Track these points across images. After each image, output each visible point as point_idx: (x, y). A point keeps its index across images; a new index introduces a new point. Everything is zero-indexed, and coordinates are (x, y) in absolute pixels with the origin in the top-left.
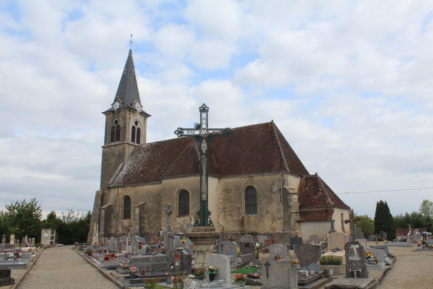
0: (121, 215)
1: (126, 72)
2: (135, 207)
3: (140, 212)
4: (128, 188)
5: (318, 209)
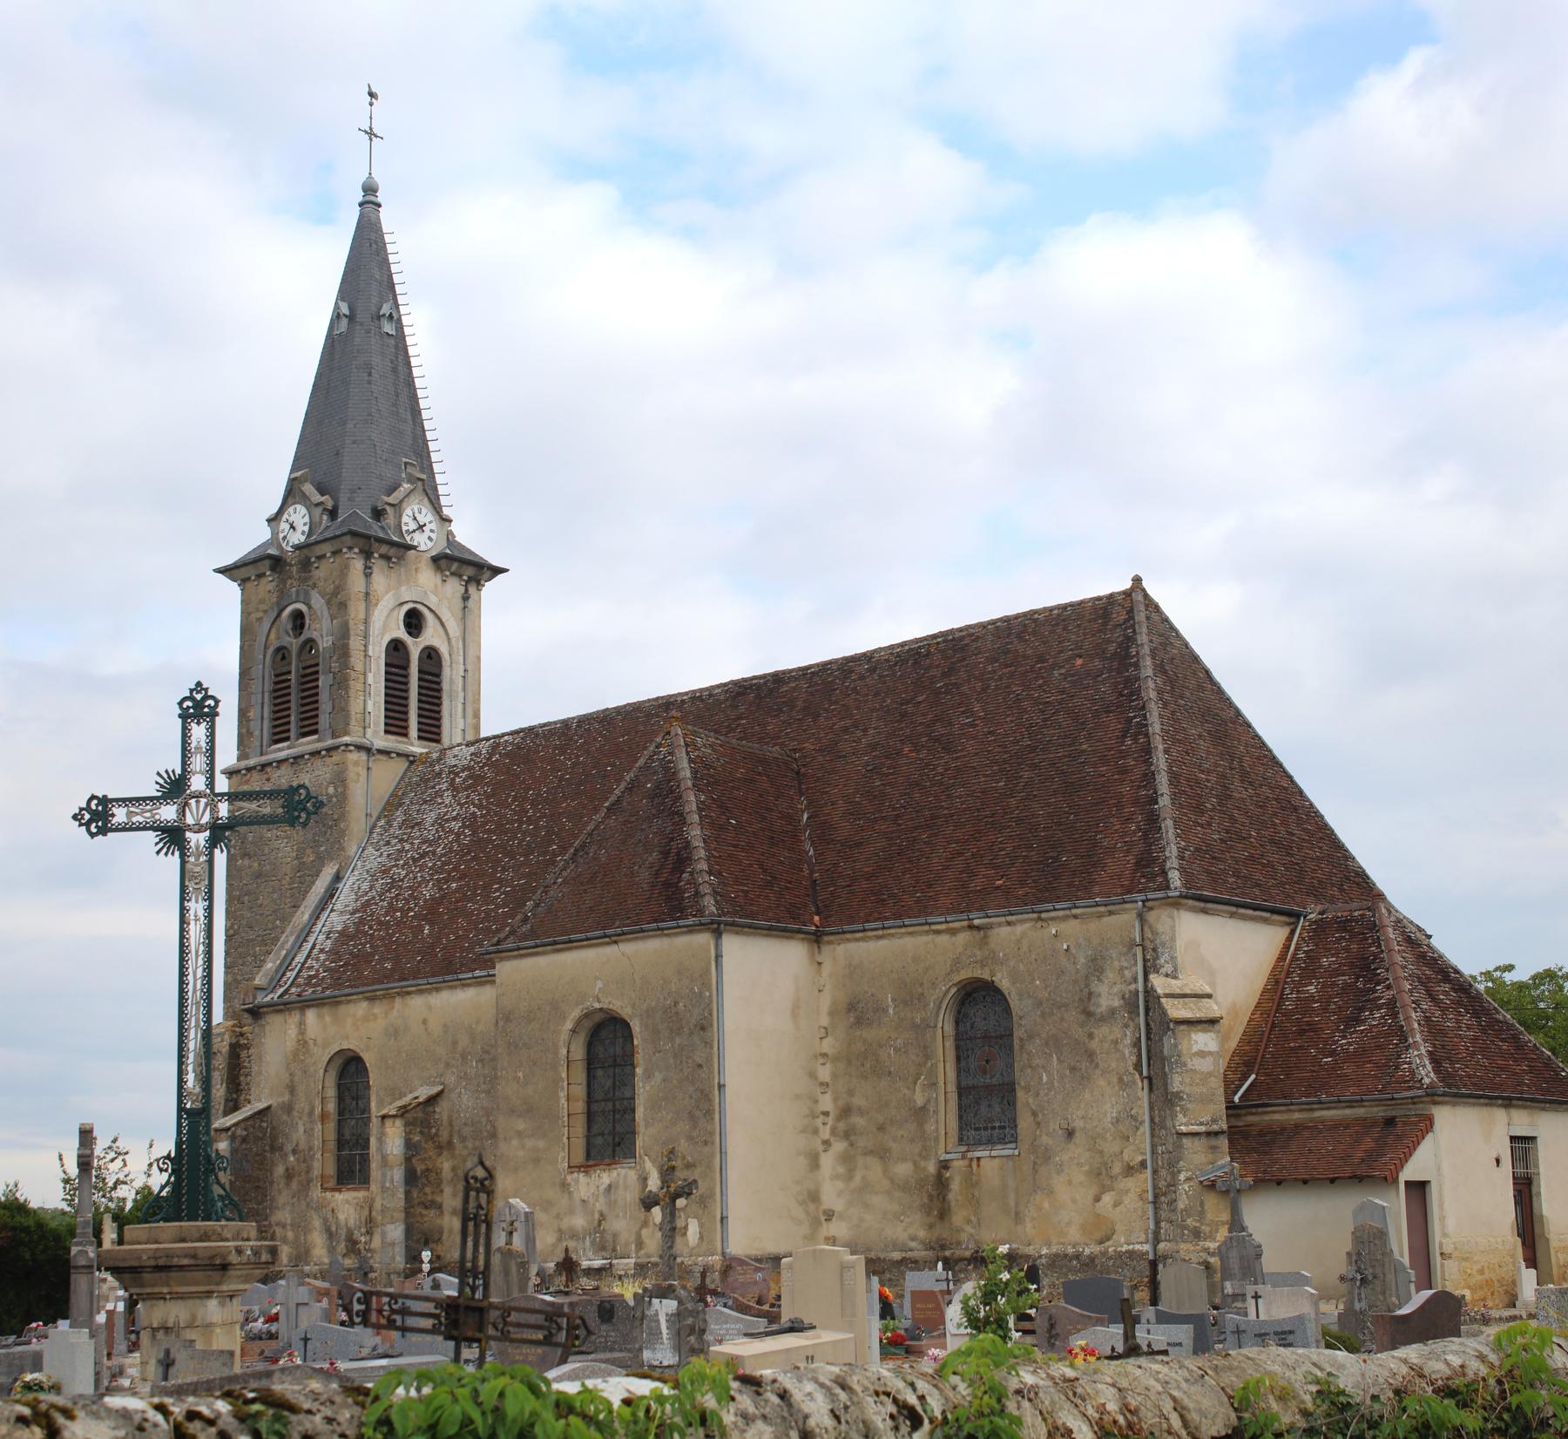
0: (324, 1163)
1: (345, 322)
2: (384, 1117)
3: (409, 1144)
4: (351, 1008)
5: (1348, 1112)
